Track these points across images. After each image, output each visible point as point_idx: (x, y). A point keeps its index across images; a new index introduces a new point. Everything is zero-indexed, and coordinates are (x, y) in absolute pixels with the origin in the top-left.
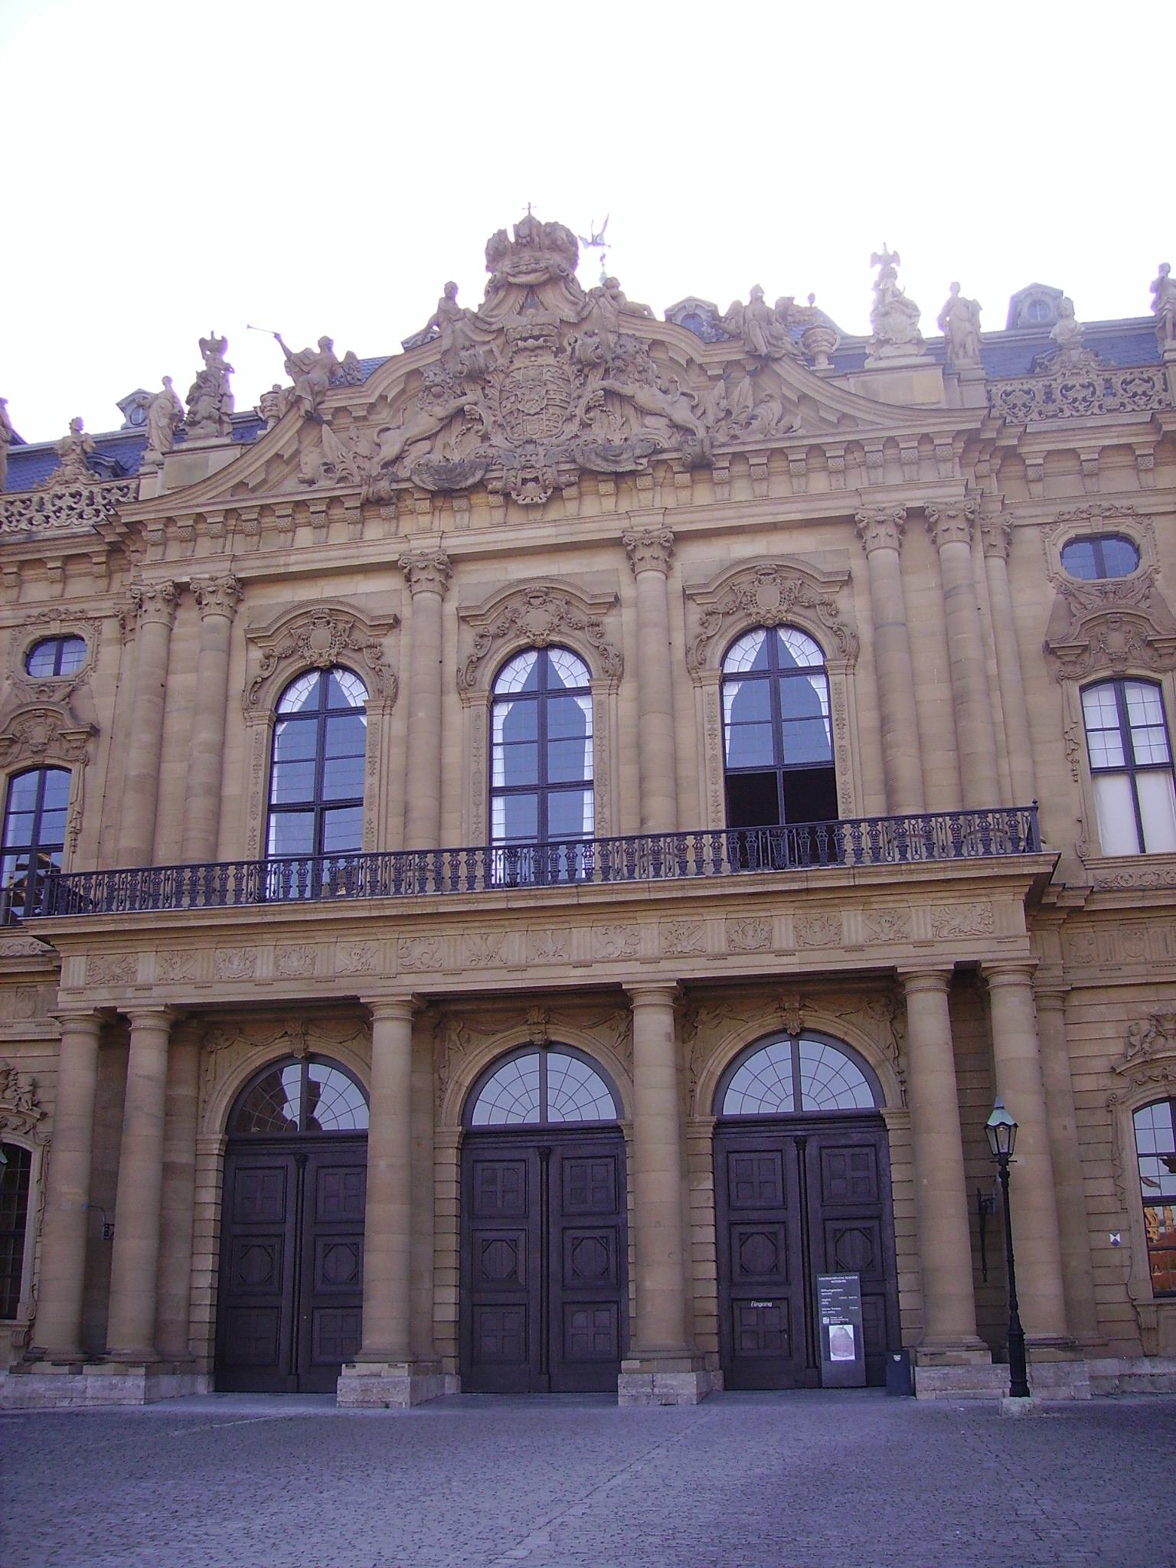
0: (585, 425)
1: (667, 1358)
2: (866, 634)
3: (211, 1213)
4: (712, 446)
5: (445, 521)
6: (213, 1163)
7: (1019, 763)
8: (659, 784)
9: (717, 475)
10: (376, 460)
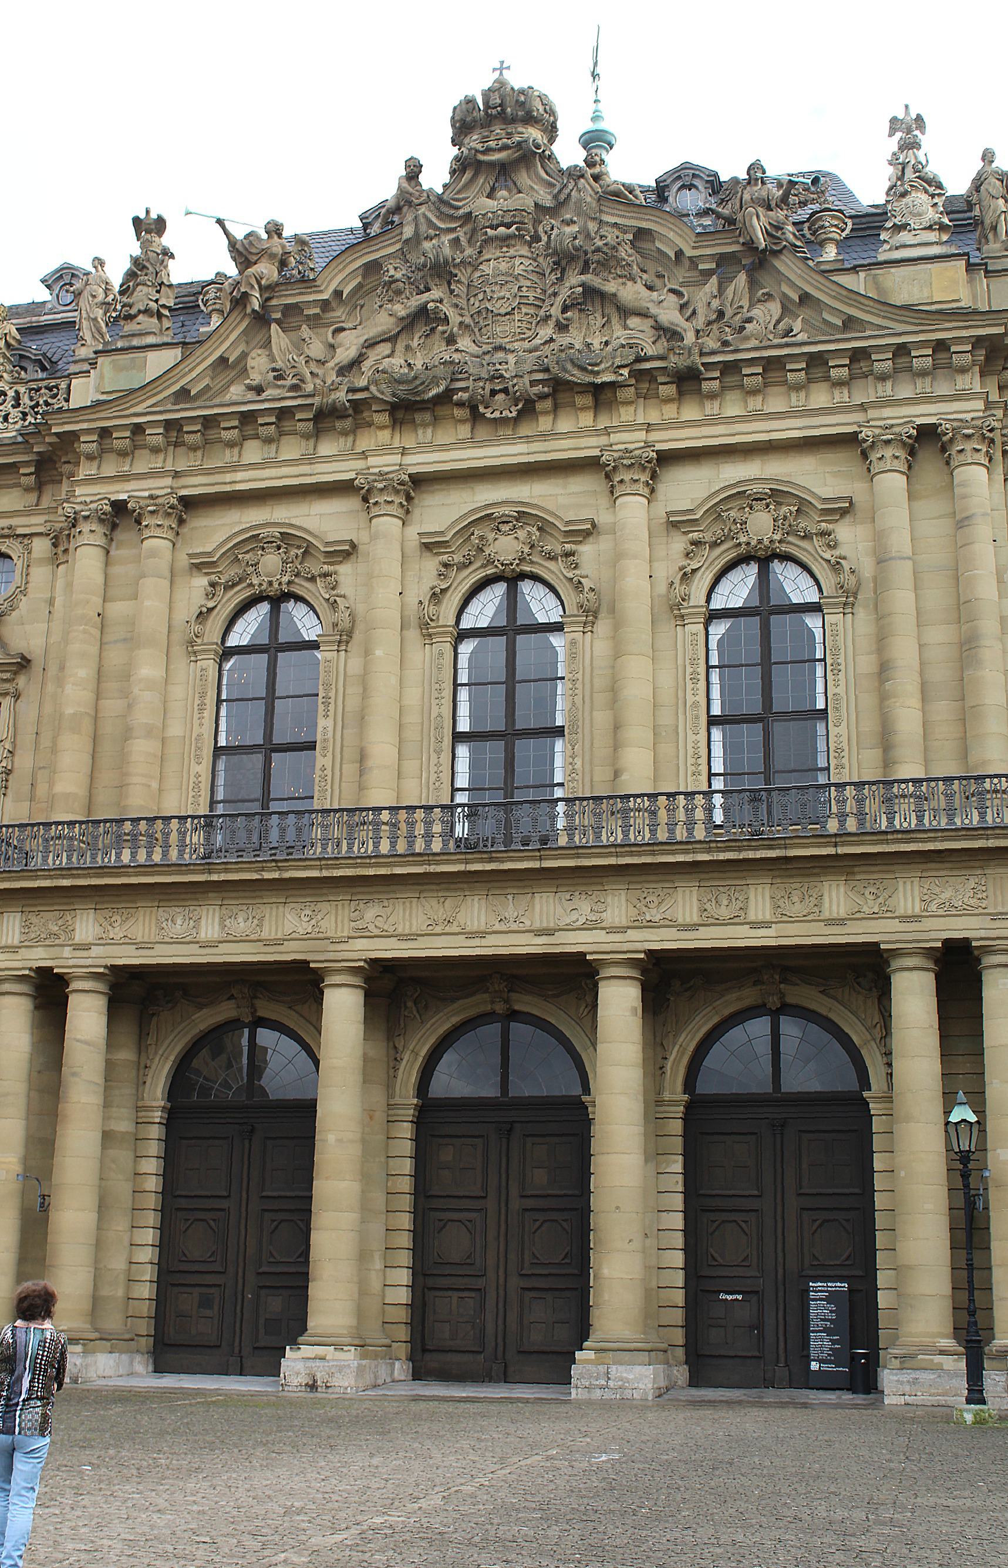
0: (562, 327)
2: (867, 568)
3: (153, 1184)
4: (702, 354)
6: (156, 1132)
9: (706, 386)
10: (331, 364)
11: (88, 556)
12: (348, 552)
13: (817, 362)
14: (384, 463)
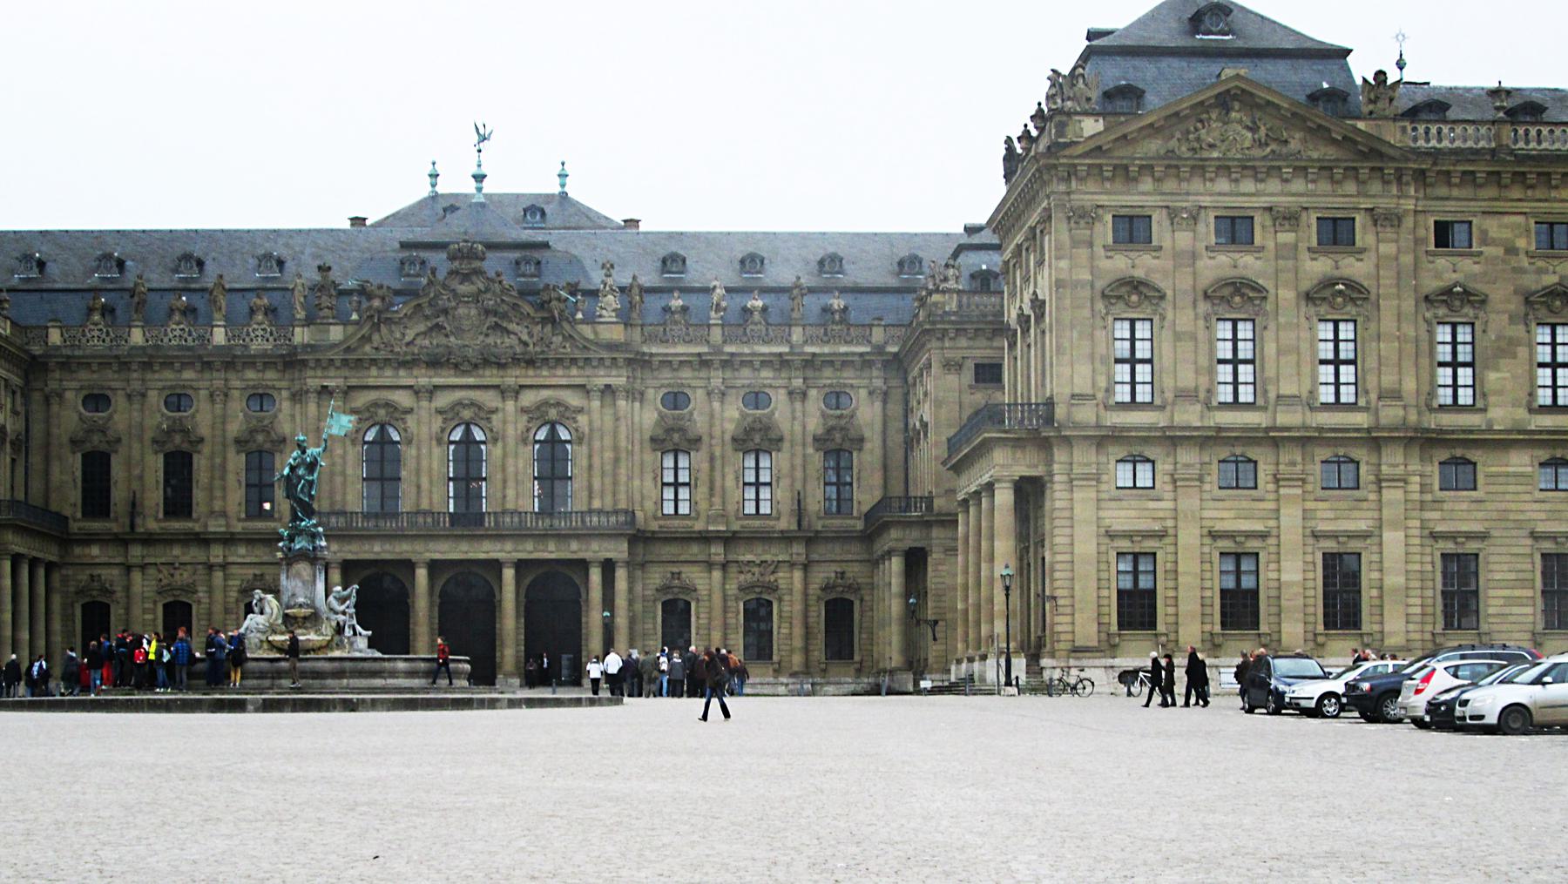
1: (512, 675)
2: (587, 430)
5: (431, 372)
7: (637, 483)
8: (511, 484)
11: (312, 408)
12: (410, 411)
13: (574, 361)
14: (423, 381)
